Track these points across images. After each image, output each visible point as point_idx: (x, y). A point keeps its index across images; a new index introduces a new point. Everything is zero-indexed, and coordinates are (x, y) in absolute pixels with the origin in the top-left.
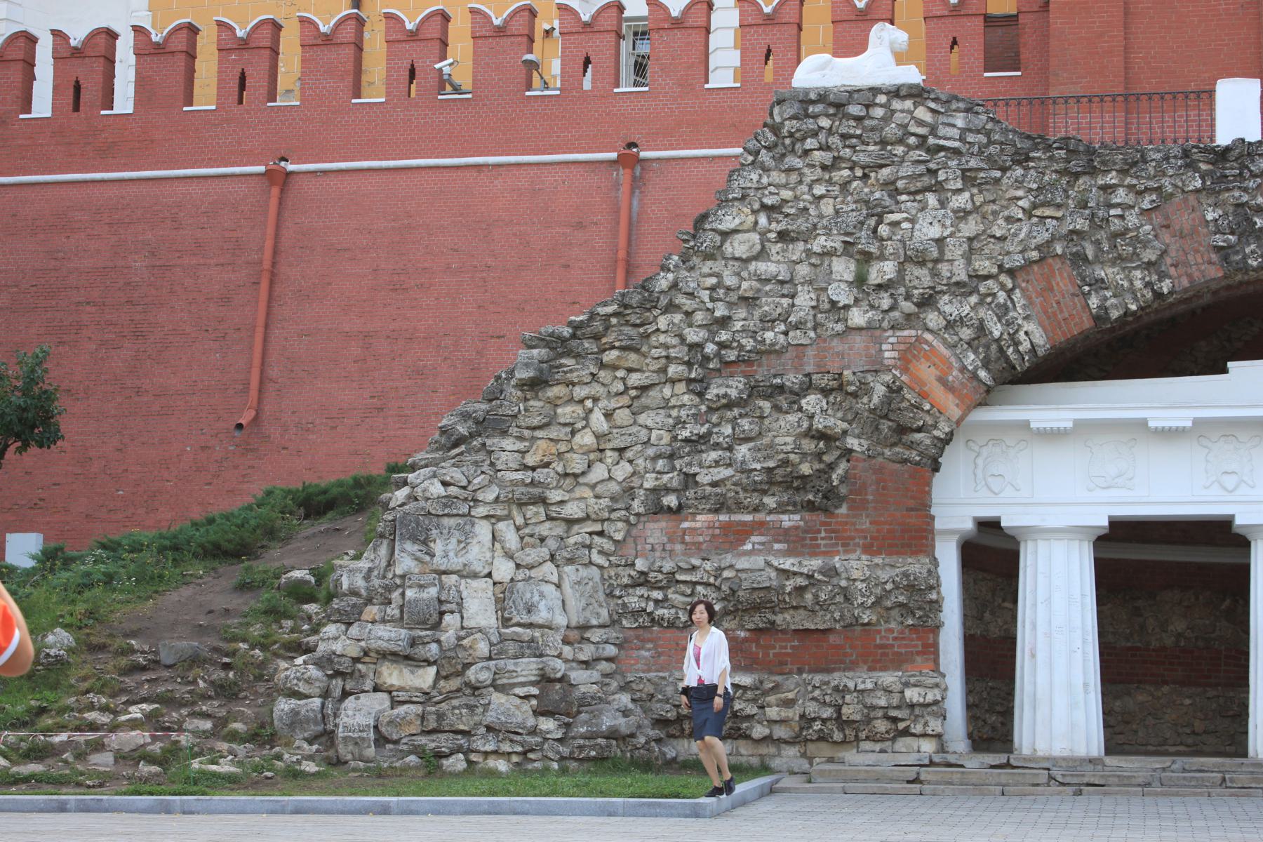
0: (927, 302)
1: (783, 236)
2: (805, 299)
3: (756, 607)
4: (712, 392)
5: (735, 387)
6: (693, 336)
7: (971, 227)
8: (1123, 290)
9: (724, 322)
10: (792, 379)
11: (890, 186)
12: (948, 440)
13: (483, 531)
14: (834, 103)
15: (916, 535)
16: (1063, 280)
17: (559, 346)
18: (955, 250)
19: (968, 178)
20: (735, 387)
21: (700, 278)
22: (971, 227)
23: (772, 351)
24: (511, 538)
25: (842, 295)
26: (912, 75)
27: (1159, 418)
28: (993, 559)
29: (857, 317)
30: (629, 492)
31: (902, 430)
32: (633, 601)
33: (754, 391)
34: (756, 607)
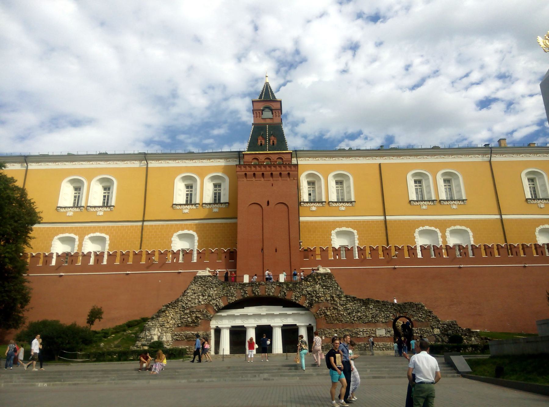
0: (210, 301)
1: (195, 293)
2: (197, 301)
3: (189, 338)
4: (186, 312)
5: (188, 311)
6: (184, 305)
7: (216, 292)
8: (233, 299)
9: (187, 304)
10: (195, 310)
11: (207, 287)
12: (212, 318)
13: (157, 329)
14: (201, 277)
15: (209, 328)
16: (226, 298)
17: (167, 306)
18: (214, 295)
19: (216, 287)
20: (188, 311)
21: (184, 298)
22: (216, 292)
23: (192, 307)
24: (160, 330)
25: (200, 300)
26: (210, 274)
27: (236, 314)
28: (218, 331)
29: (202, 303)
30: (175, 324)
31: (207, 316)
32: (175, 338)
33: (190, 312)
34: (189, 338)
